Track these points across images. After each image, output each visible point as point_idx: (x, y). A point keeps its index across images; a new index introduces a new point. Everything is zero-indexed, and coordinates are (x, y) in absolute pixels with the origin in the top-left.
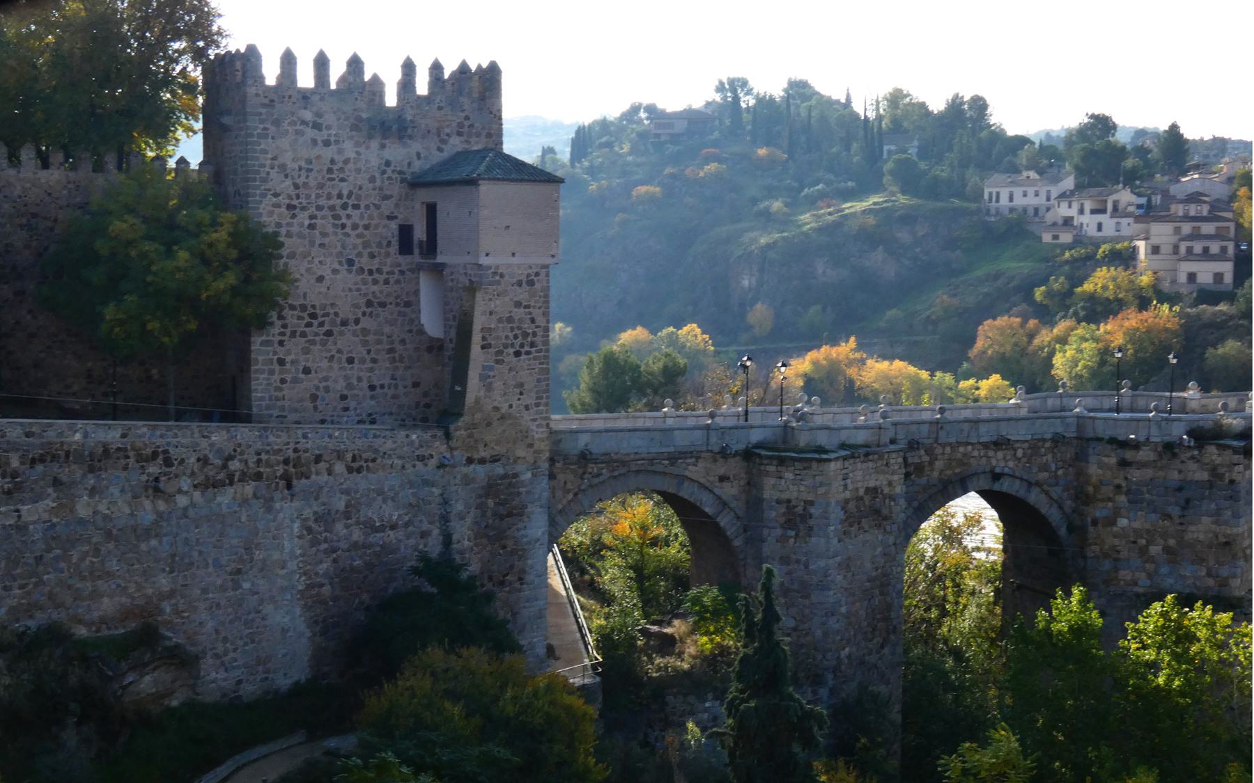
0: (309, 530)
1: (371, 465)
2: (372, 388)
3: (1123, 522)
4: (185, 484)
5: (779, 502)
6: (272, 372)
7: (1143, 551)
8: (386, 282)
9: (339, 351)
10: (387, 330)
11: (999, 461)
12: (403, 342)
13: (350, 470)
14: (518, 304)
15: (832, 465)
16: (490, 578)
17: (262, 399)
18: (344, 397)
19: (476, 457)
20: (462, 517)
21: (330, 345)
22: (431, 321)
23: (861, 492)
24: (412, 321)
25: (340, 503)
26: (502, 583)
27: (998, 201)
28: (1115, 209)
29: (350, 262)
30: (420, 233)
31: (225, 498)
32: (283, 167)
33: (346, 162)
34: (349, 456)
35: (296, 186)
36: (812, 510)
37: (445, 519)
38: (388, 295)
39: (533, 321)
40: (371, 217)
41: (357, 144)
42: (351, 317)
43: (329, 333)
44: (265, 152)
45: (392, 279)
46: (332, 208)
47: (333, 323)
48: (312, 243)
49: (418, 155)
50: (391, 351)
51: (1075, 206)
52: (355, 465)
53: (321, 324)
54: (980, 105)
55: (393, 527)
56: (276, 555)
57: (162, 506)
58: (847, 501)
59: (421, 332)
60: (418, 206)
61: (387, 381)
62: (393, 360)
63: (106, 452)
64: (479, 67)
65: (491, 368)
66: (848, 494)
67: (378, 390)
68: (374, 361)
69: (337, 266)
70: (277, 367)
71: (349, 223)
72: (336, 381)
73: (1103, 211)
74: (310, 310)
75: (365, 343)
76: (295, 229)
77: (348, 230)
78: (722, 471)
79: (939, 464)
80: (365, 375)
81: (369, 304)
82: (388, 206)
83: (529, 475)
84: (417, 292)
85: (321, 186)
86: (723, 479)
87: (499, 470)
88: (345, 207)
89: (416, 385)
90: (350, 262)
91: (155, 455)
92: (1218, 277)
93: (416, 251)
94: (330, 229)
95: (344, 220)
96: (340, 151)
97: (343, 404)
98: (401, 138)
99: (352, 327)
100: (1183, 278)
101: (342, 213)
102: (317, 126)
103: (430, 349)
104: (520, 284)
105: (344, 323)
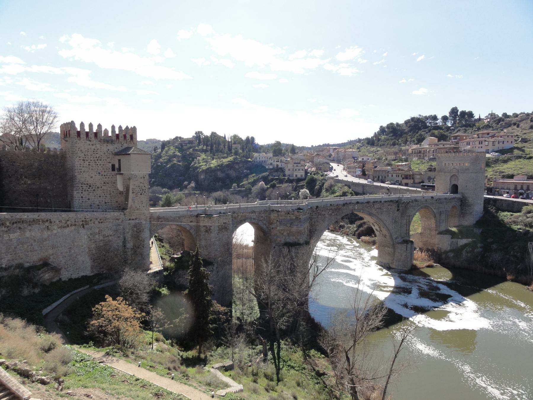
0: (89, 237)
1: (105, 221)
2: (106, 203)
3: (278, 228)
4: (55, 227)
5: (204, 226)
6: (79, 200)
7: (282, 234)
8: (109, 178)
9: (97, 194)
10: (109, 189)
11: (252, 215)
12: (113, 192)
13: (99, 223)
14: (141, 183)
15: (216, 218)
16: (136, 247)
17: (77, 206)
18: (98, 205)
20: (128, 233)
21: (95, 193)
22: (120, 187)
24: (115, 187)
25: (97, 230)
26: (139, 248)
28: (281, 161)
29: (99, 173)
30: (117, 166)
31: (67, 231)
32: (81, 151)
33: (98, 149)
34: (99, 220)
35: (85, 155)
36: (211, 228)
37: (124, 233)
38: (109, 181)
39: (145, 186)
40: (104, 162)
41: (101, 145)
42: (100, 186)
44: (77, 147)
45: (110, 177)
46: (94, 160)
47: (95, 188)
48: (89, 169)
49: (116, 148)
50: (110, 194)
51: (273, 160)
52: (101, 221)
53: (92, 188)
54: (253, 138)
55: (110, 236)
56: (81, 244)
57: (49, 233)
58: (219, 226)
59: (118, 189)
60: (116, 160)
61: (109, 201)
62: (111, 196)
63: (34, 220)
64: (127, 127)
65: (135, 198)
67: (107, 204)
68: (106, 196)
69: (96, 174)
70: (81, 199)
71: (99, 164)
72: (96, 202)
73: (279, 162)
74: (89, 185)
75: (103, 192)
77: (99, 165)
78: (191, 220)
79: (239, 217)
80: (104, 200)
81: (104, 183)
82: (108, 160)
84: (116, 180)
85: (91, 155)
87: (137, 221)
88: (98, 160)
89: (117, 202)
90: (99, 173)
91: (47, 221)
92: (302, 176)
93: (116, 170)
94: (94, 166)
95: (97, 163)
96: (96, 147)
97: (98, 207)
98: (112, 144)
99: (100, 189)
100: (295, 176)
101: (97, 161)
103: (120, 194)
104: (141, 178)
105: (98, 188)
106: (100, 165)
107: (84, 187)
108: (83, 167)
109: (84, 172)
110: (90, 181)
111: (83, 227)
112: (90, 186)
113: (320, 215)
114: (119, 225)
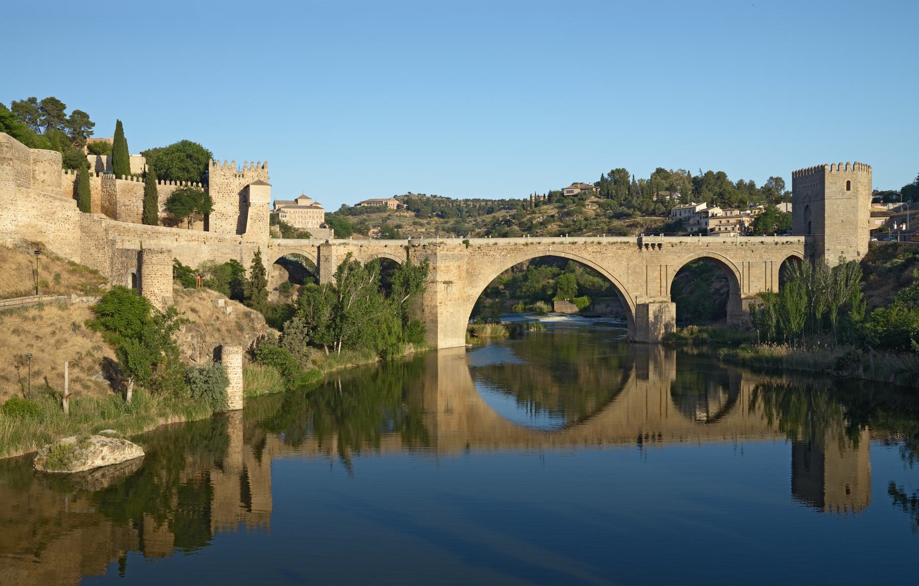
0: (209, 252)
14: (260, 211)
19: (249, 241)
23: (343, 254)
27: (676, 216)
29: (232, 204)
31: (191, 244)
34: (218, 239)
37: (241, 254)
43: (227, 219)
48: (223, 200)
55: (228, 254)
66: (338, 254)
76: (219, 197)
79: (370, 251)
83: (262, 247)
85: (225, 188)
86: (313, 252)
90: (232, 204)
91: (176, 234)
99: (232, 217)
102: (224, 175)
105: (230, 217)
106: (233, 196)
107: (218, 215)
108: (218, 198)
109: (218, 202)
110: (224, 211)
111: (205, 243)
112: (223, 215)
113: (487, 255)
114: (236, 246)
